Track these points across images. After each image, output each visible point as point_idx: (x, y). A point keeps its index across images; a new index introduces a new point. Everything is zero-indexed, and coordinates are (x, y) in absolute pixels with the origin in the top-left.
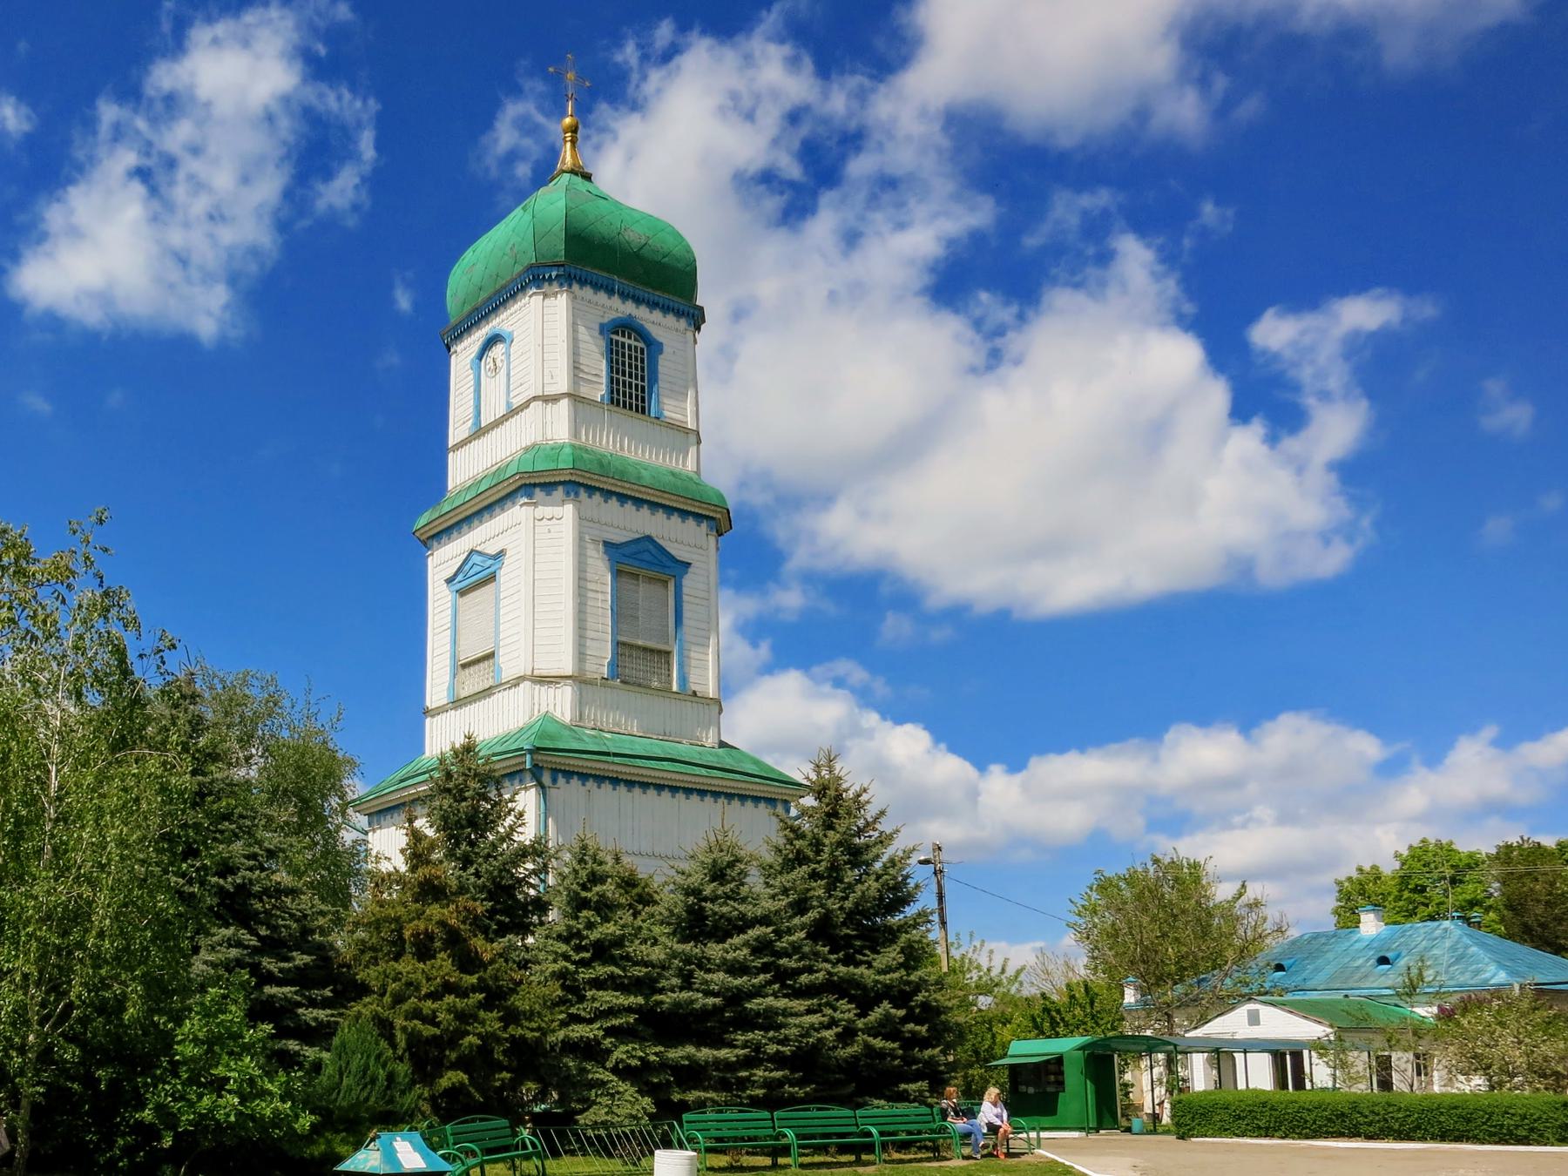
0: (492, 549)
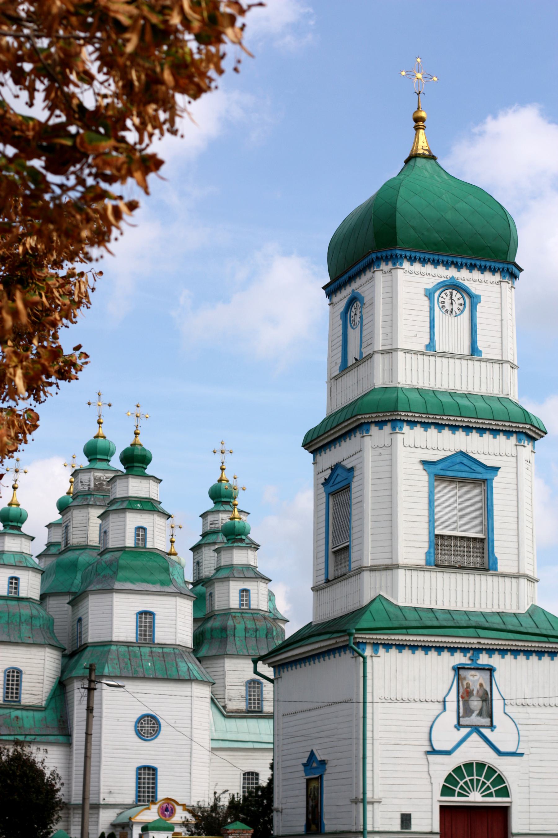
0: (349, 466)
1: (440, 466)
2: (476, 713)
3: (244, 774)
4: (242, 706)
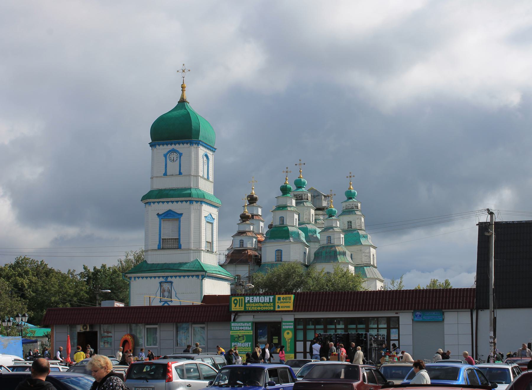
1: (163, 216)
2: (166, 297)
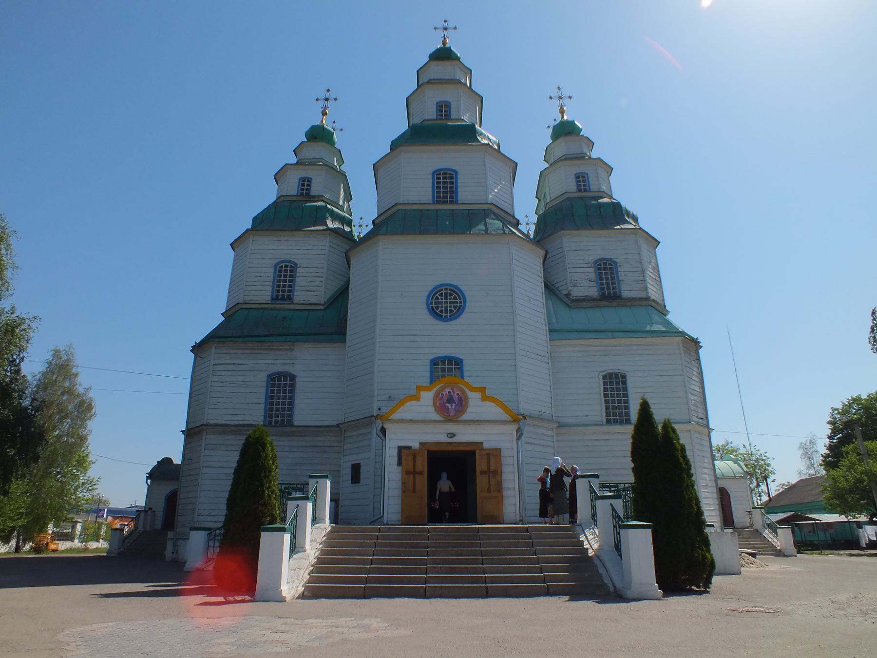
3: (604, 377)
4: (593, 291)
